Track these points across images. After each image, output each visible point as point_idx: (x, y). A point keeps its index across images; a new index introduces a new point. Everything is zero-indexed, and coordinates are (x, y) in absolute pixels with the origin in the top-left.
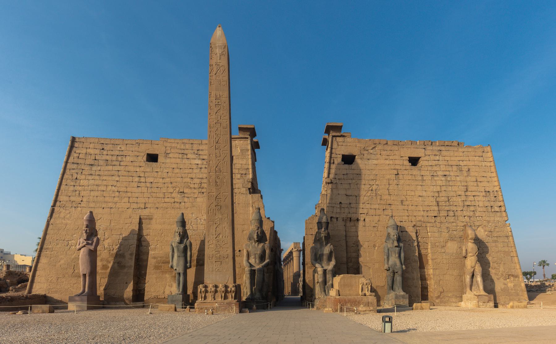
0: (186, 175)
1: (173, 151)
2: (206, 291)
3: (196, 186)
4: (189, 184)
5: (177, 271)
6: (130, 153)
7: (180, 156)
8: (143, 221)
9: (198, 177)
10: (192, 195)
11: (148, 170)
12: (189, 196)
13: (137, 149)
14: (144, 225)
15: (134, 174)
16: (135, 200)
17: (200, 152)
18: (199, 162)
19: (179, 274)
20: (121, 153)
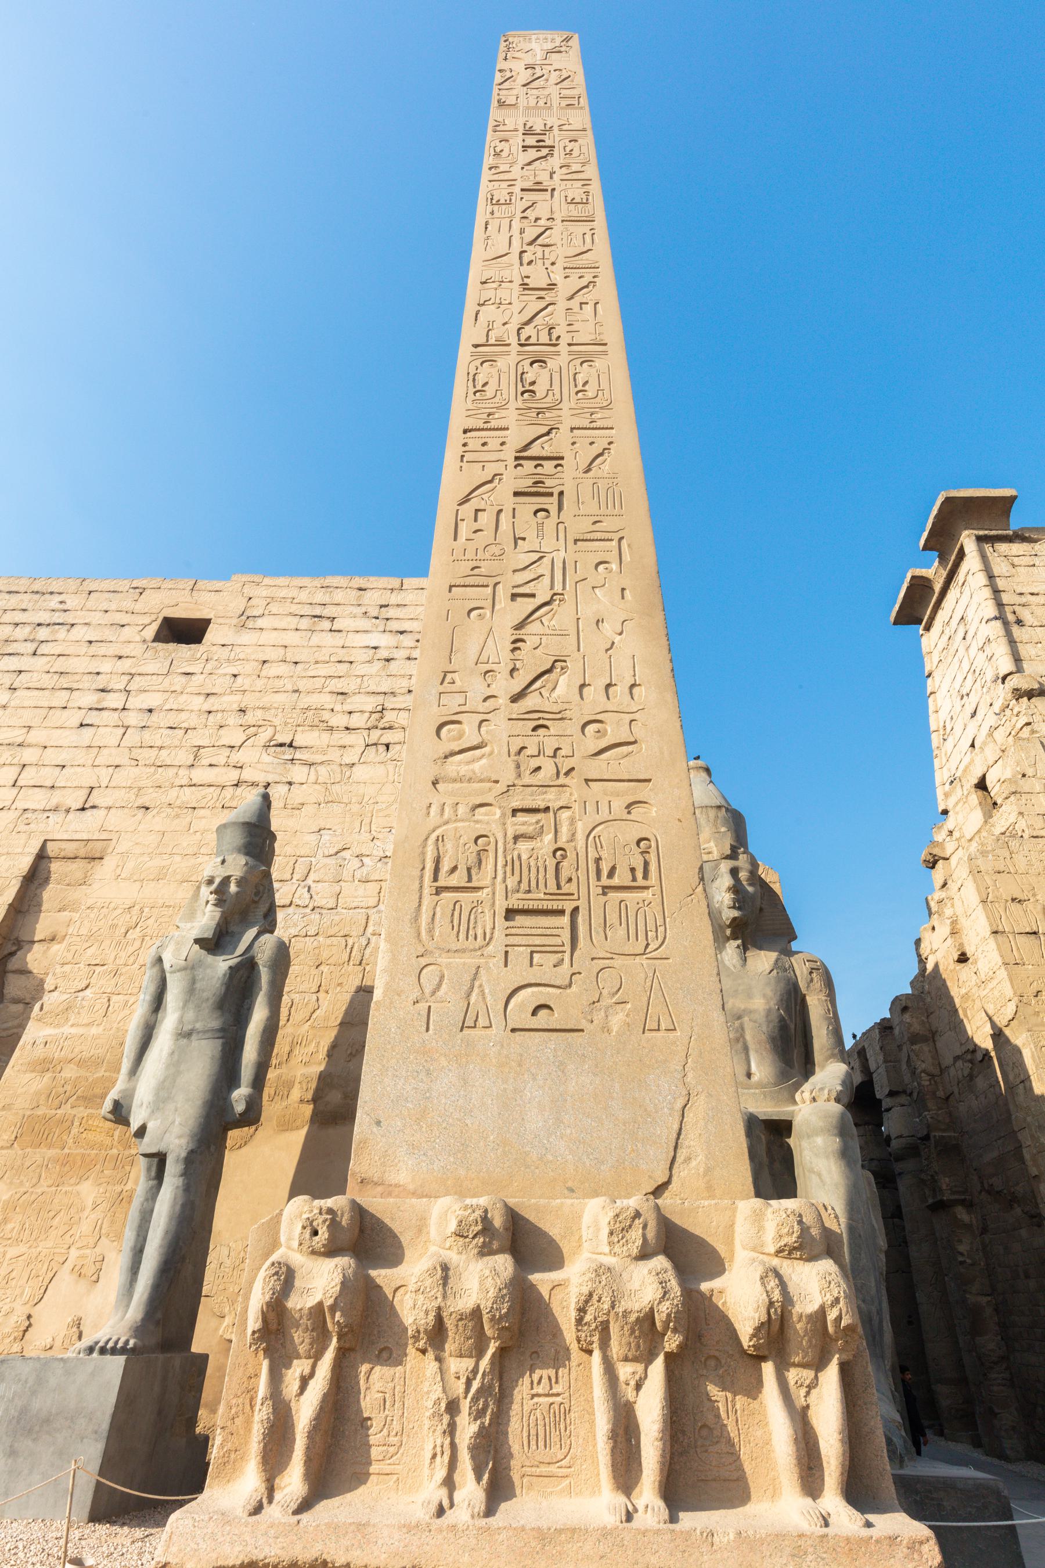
0: (318, 683)
1: (274, 608)
2: (365, 1328)
3: (356, 721)
4: (326, 715)
5: (148, 1144)
6: (97, 618)
7: (305, 623)
8: (55, 866)
9: (373, 688)
10: (334, 755)
11: (150, 668)
12: (318, 758)
13: (128, 604)
14: (50, 895)
15: (87, 682)
16: (48, 776)
17: (391, 613)
18: (385, 641)
19: (159, 1160)
20: (58, 618)
